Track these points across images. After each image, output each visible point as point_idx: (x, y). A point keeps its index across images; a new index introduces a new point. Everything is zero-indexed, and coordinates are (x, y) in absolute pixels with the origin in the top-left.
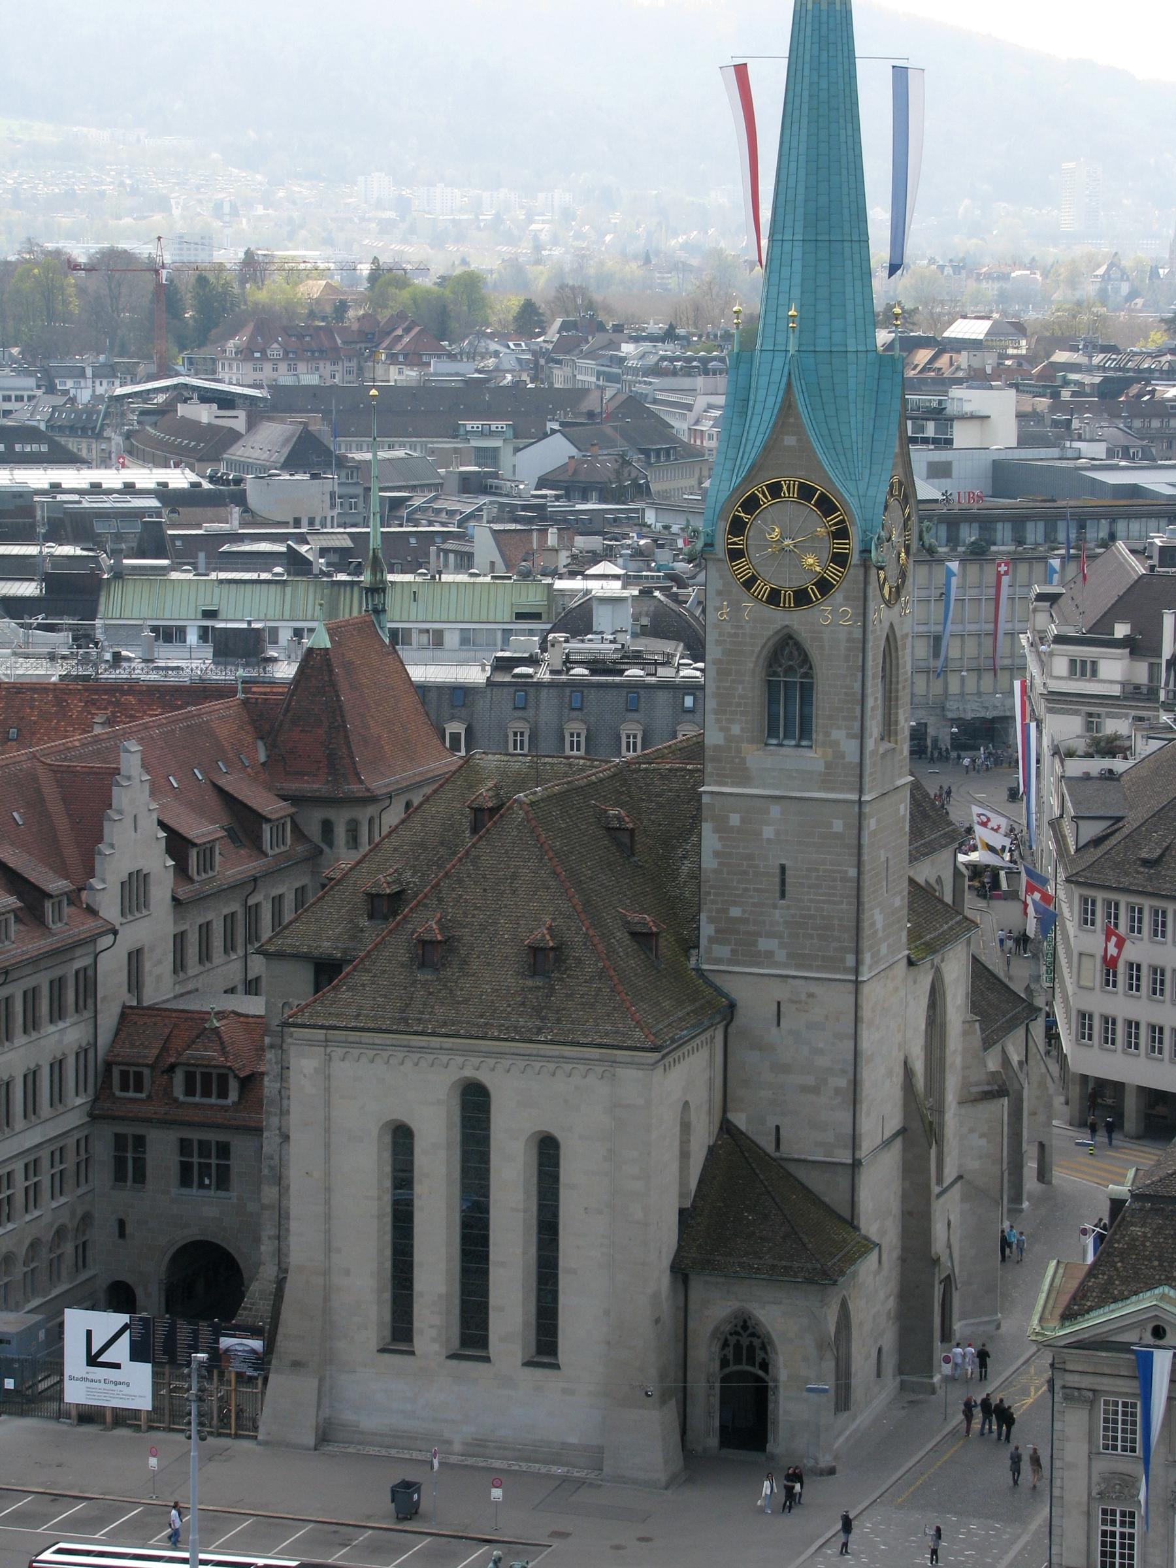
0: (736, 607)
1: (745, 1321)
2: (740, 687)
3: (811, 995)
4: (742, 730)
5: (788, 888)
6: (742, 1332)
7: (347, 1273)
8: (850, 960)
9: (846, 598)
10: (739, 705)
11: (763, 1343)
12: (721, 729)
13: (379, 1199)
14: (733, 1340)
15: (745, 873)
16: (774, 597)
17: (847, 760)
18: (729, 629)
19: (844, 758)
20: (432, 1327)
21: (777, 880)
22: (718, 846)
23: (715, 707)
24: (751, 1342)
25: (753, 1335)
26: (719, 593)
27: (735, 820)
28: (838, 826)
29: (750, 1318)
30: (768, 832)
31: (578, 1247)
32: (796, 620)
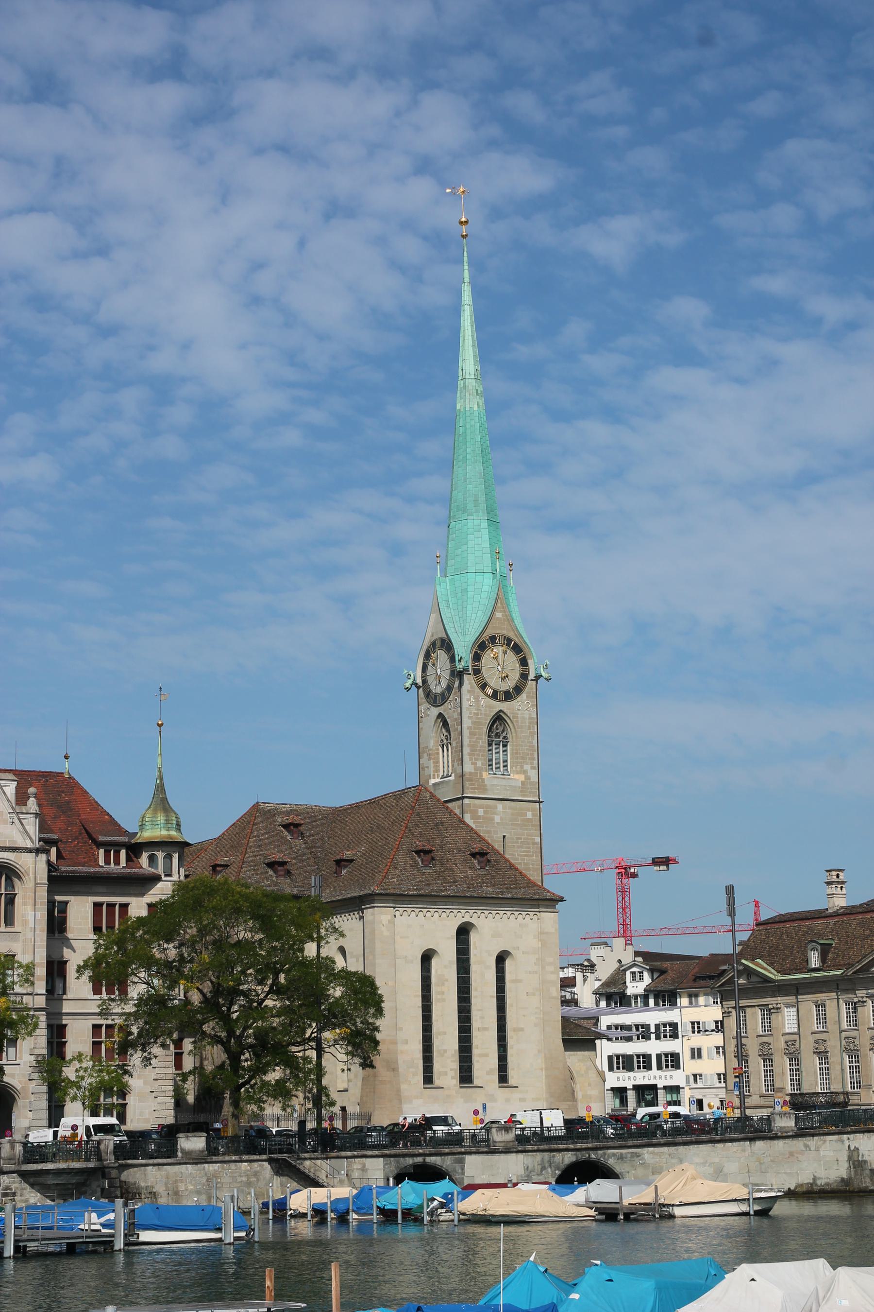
0: (477, 699)
4: (482, 764)
7: (406, 1042)
9: (527, 697)
10: (480, 751)
12: (472, 763)
16: (495, 696)
17: (532, 780)
18: (474, 710)
19: (530, 779)
20: (451, 1070)
21: (502, 844)
23: (469, 751)
26: (469, 691)
27: (481, 812)
28: (529, 815)
30: (497, 819)
31: (524, 1016)
32: (504, 706)
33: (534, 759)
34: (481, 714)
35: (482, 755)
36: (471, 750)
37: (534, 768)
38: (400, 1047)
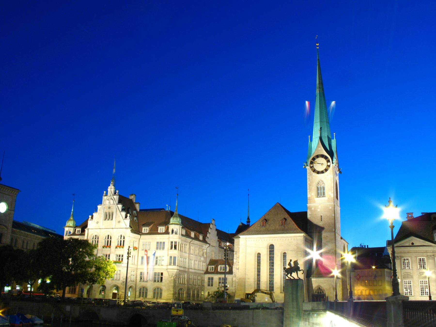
1: (319, 288)
2: (313, 187)
3: (327, 236)
5: (322, 219)
6: (319, 289)
8: (334, 230)
11: (323, 291)
12: (310, 194)
13: (255, 265)
14: (317, 291)
15: (315, 217)
17: (331, 197)
20: (264, 287)
22: (310, 213)
24: (321, 291)
25: (321, 290)
29: (320, 286)
30: (319, 210)
33: (332, 190)
34: (313, 179)
35: (314, 191)
36: (310, 190)
37: (333, 193)
38: (247, 280)
